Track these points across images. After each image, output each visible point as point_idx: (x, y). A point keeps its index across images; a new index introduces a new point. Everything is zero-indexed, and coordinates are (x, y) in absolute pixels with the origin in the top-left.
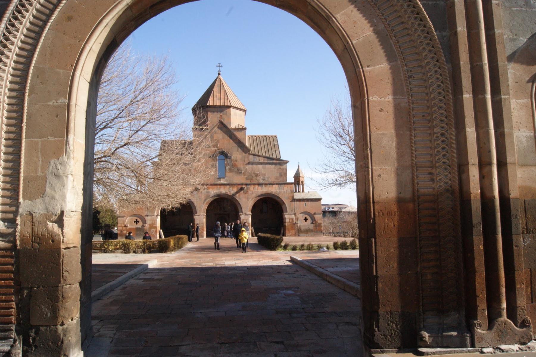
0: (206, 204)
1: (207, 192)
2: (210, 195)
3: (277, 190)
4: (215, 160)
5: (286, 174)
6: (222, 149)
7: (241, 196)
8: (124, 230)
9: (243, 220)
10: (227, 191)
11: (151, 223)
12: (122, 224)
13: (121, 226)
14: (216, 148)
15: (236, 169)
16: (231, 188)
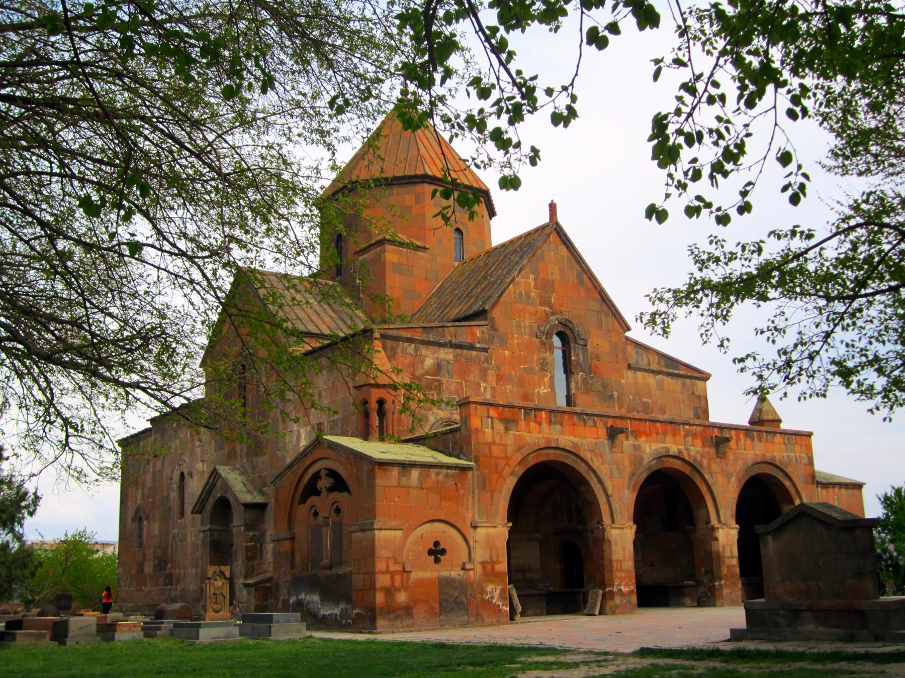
0: (633, 488)
1: (634, 446)
2: (642, 459)
3: (784, 454)
4: (547, 346)
5: (705, 412)
6: (561, 313)
7: (714, 467)
8: (398, 590)
9: (724, 546)
10: (681, 447)
11: (486, 557)
12: (391, 562)
13: (387, 572)
14: (548, 309)
15: (600, 383)
16: (689, 439)
